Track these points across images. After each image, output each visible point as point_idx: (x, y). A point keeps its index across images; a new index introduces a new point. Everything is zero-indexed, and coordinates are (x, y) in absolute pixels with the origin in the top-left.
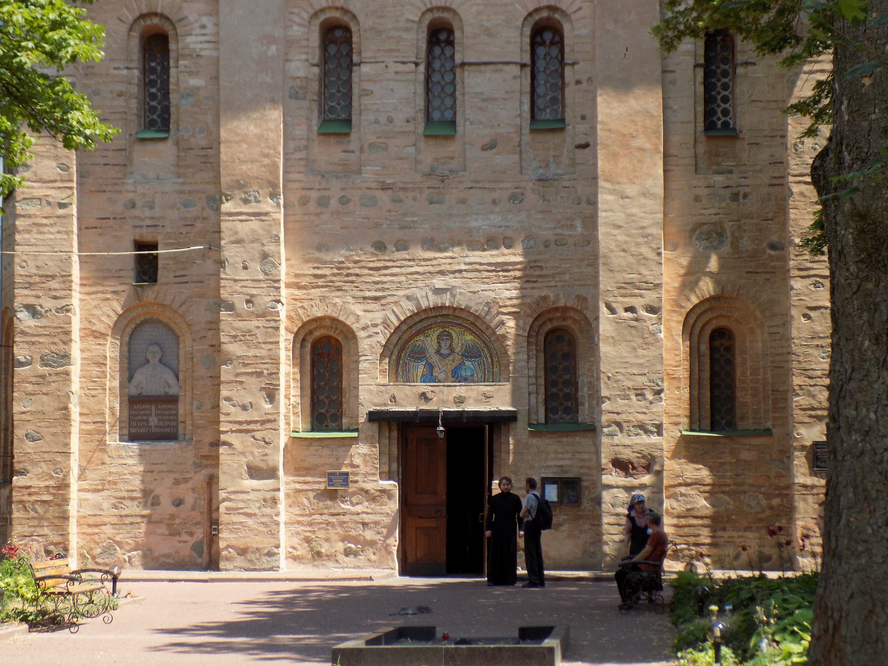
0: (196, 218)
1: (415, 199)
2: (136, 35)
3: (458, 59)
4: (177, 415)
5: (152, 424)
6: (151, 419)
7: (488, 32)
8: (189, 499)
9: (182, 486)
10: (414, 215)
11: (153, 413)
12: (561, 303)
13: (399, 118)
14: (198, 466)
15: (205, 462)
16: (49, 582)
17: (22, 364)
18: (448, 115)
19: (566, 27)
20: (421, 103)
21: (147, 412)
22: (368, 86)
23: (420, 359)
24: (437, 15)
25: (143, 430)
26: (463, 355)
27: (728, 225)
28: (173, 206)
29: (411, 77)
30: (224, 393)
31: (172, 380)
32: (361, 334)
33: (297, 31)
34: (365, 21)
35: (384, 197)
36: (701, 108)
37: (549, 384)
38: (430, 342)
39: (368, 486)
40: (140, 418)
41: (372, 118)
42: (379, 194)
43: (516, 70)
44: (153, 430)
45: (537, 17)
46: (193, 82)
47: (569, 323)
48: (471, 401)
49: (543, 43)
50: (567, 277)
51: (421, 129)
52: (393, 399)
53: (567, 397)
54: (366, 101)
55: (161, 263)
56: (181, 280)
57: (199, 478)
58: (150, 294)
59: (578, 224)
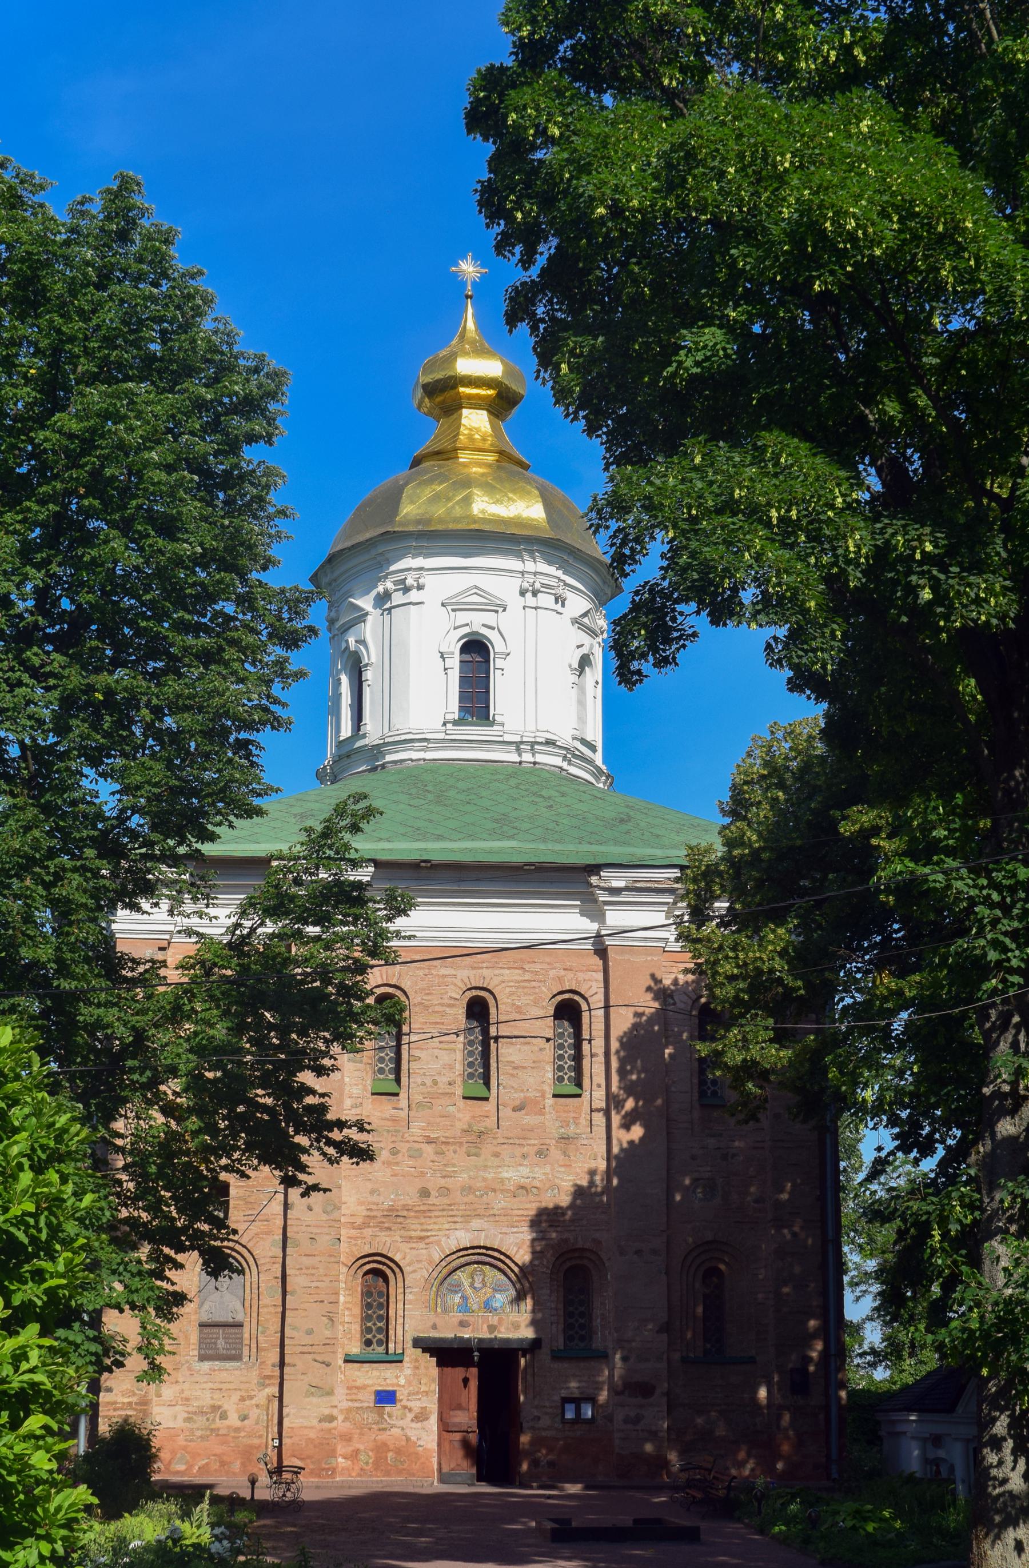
1: (455, 1152)
4: (242, 1338)
9: (247, 1402)
10: (454, 1165)
12: (580, 1245)
13: (443, 1080)
15: (267, 1382)
23: (456, 1292)
24: (475, 993)
25: (212, 1352)
26: (494, 1290)
29: (452, 1046)
31: (238, 1306)
34: (415, 998)
35: (429, 1149)
36: (696, 1081)
39: (409, 1404)
41: (419, 1080)
42: (425, 1146)
45: (560, 998)
48: (503, 1329)
50: (584, 1222)
52: (434, 1327)
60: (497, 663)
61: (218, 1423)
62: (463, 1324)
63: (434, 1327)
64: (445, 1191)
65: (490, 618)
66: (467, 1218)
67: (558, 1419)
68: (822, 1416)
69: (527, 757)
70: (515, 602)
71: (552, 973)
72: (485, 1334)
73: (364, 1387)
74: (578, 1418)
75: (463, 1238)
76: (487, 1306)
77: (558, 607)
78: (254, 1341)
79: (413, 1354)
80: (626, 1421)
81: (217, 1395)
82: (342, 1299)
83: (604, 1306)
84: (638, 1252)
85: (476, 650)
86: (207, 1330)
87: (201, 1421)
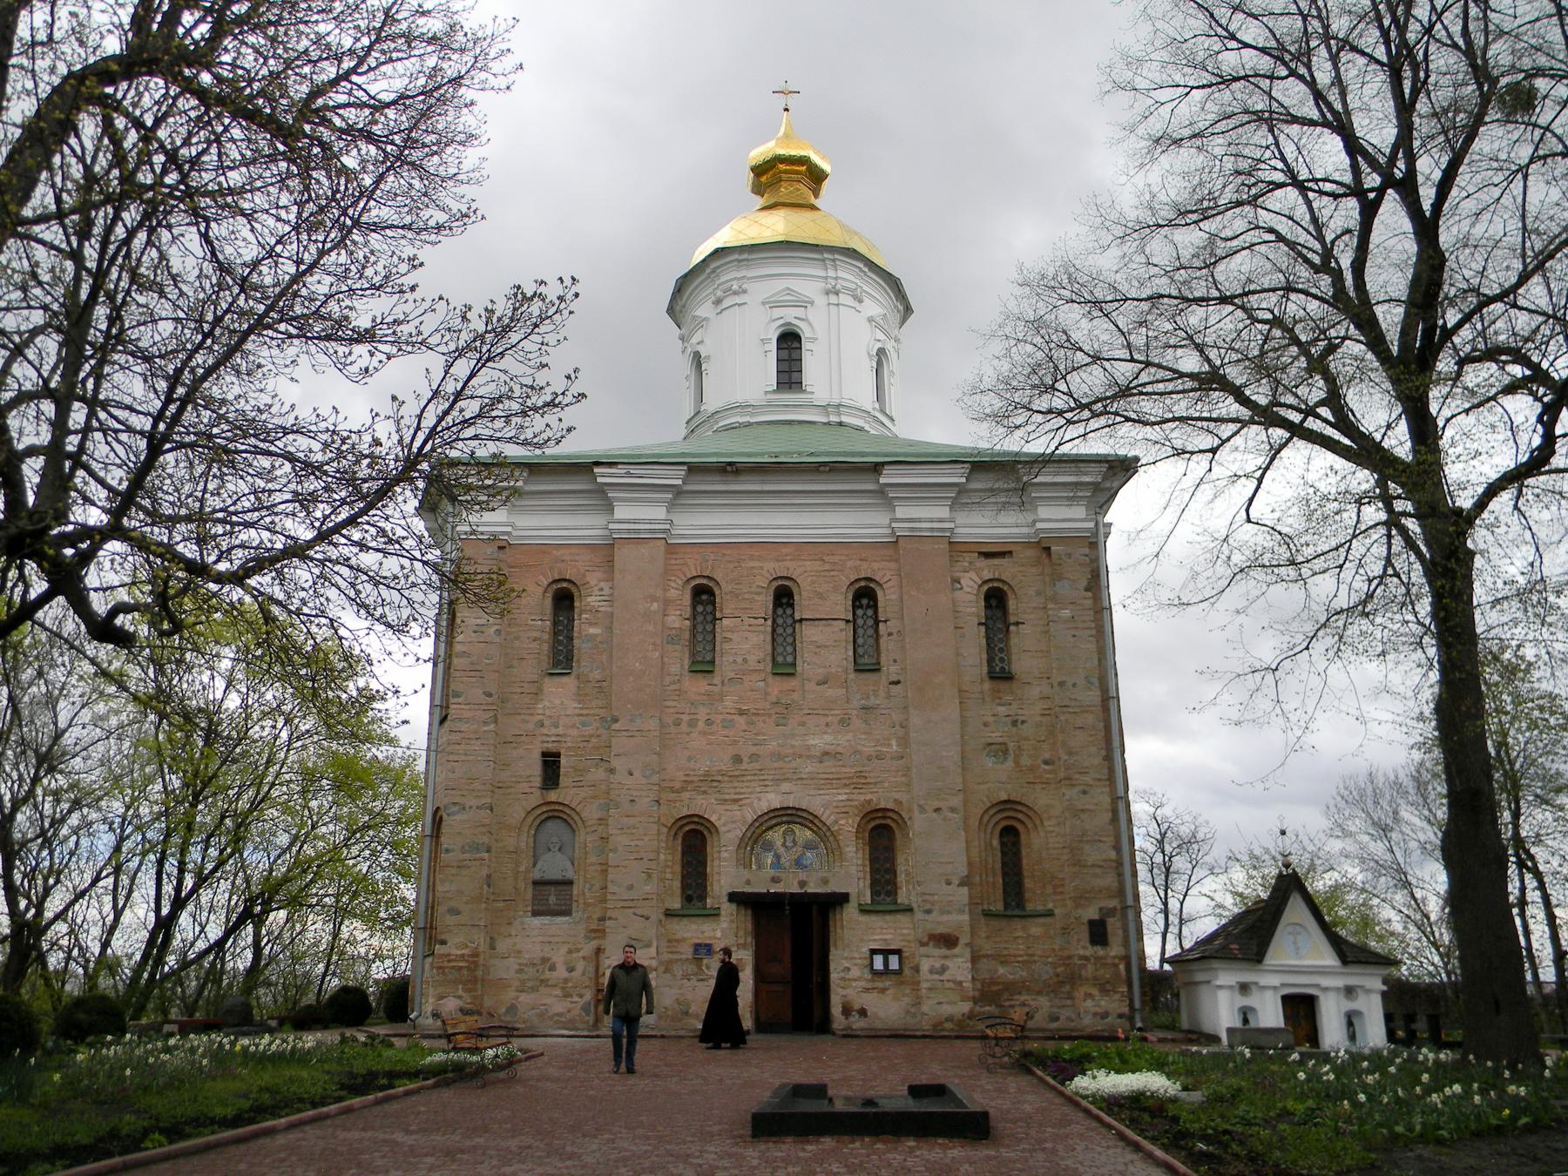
0: (591, 736)
2: (549, 595)
3: (797, 617)
7: (820, 596)
8: (580, 966)
13: (752, 659)
14: (588, 938)
16: (460, 1037)
17: (447, 851)
18: (790, 659)
19: (880, 593)
20: (769, 648)
22: (729, 635)
27: (1011, 745)
28: (574, 726)
30: (610, 877)
31: (568, 864)
32: (722, 829)
33: (673, 593)
35: (741, 720)
36: (985, 656)
37: (873, 871)
38: (776, 836)
42: (736, 717)
43: (842, 624)
46: (592, 631)
47: (888, 821)
49: (861, 607)
51: (769, 668)
53: (888, 882)
54: (726, 646)
55: (562, 770)
56: (578, 784)
57: (588, 948)
58: (553, 796)
59: (894, 742)
60: (805, 345)
61: (548, 974)
62: (775, 880)
63: (748, 882)
64: (754, 757)
65: (800, 312)
66: (778, 781)
67: (867, 971)
68: (1122, 967)
69: (834, 419)
70: (821, 300)
71: (849, 564)
72: (795, 889)
73: (684, 940)
74: (887, 971)
75: (772, 799)
76: (798, 863)
77: (855, 304)
79: (728, 909)
80: (931, 972)
81: (547, 948)
82: (662, 857)
83: (905, 863)
84: (937, 810)
85: (790, 341)
87: (531, 971)
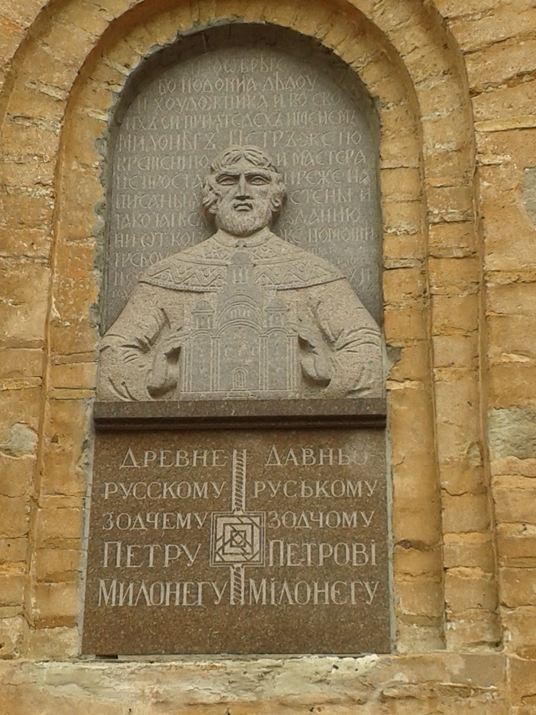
4: (375, 504)
5: (232, 554)
6: (222, 526)
11: (239, 494)
21: (200, 490)
25: (175, 595)
31: (347, 313)
40: (158, 521)
44: (238, 591)
78: (460, 514)
86: (147, 457)
